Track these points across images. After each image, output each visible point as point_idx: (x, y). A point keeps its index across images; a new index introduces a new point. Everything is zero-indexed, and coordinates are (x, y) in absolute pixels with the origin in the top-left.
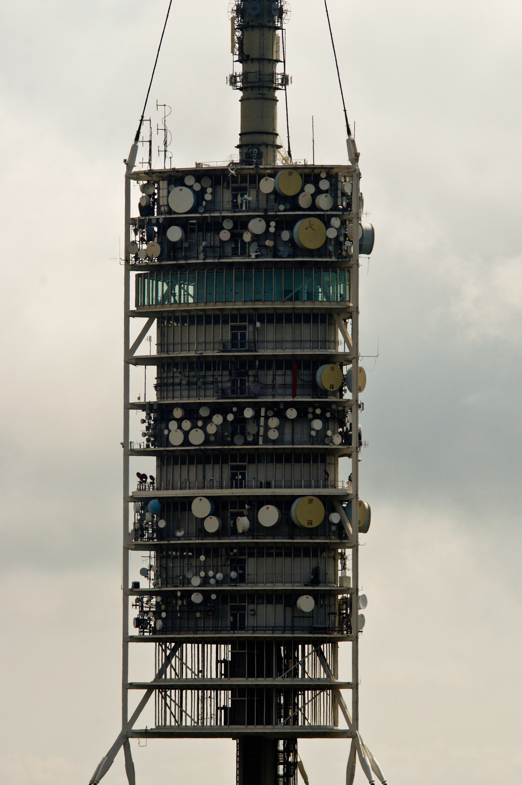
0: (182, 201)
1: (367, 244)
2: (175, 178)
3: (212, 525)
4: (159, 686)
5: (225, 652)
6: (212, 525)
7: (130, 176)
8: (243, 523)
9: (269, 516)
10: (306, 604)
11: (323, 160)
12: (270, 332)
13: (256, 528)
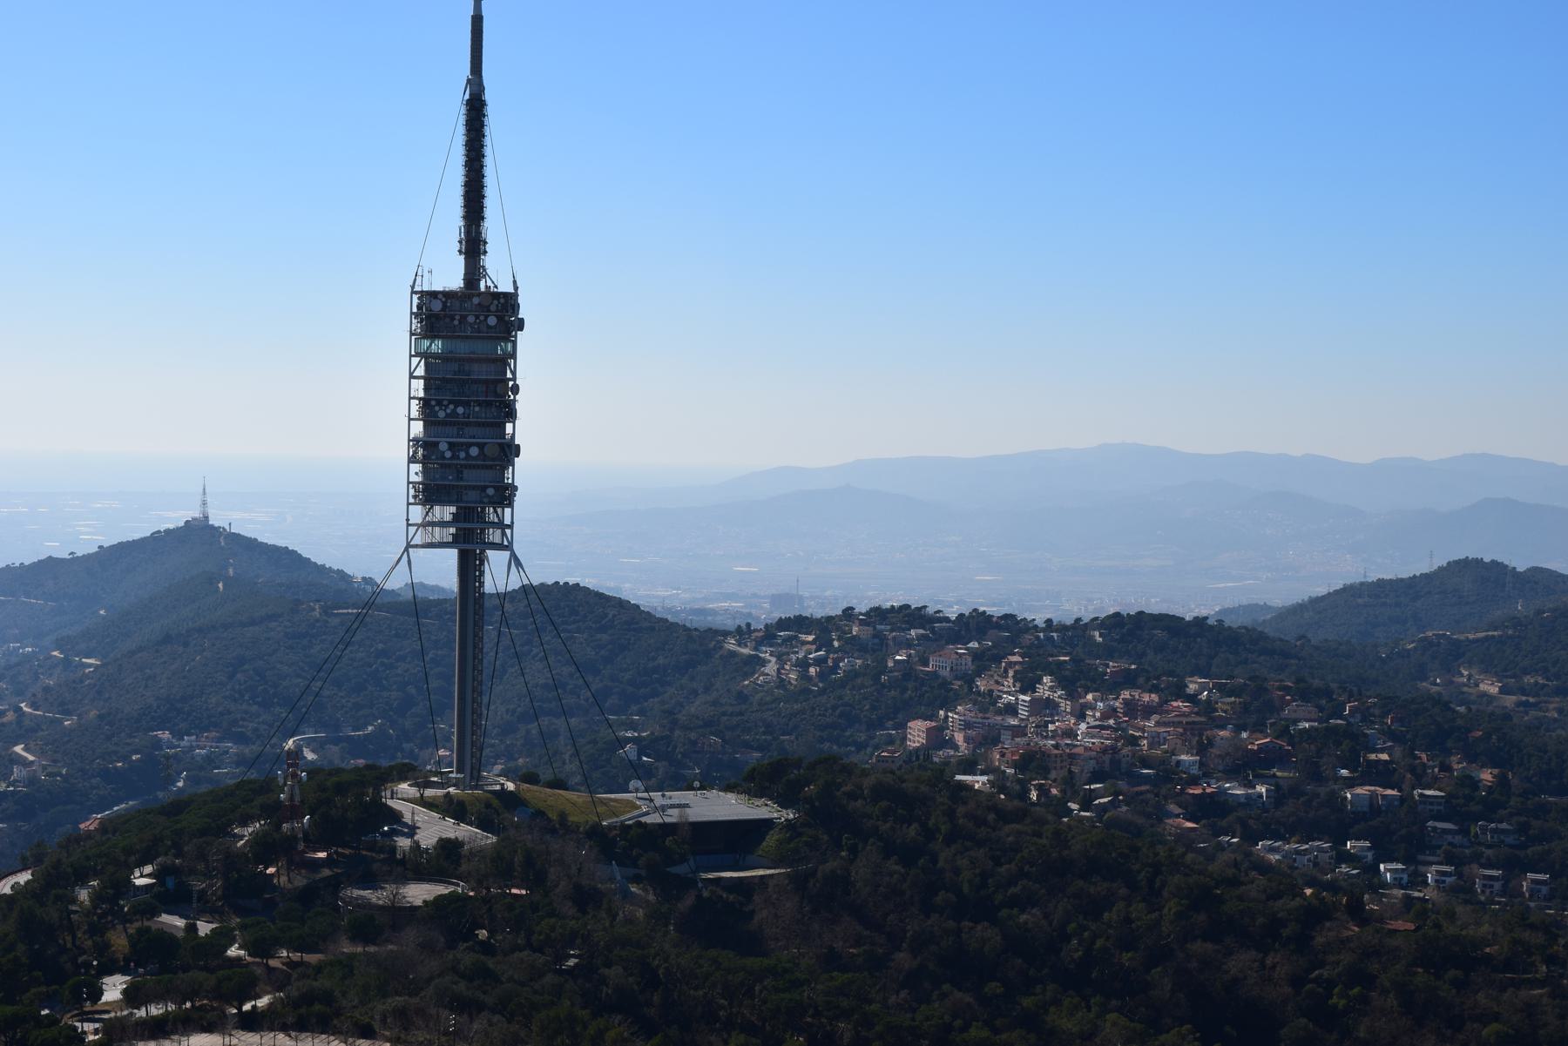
0: (437, 306)
1: (520, 325)
2: (433, 295)
3: (448, 454)
4: (425, 525)
5: (453, 509)
6: (448, 454)
7: (413, 292)
8: (462, 455)
9: (474, 451)
10: (491, 491)
11: (500, 290)
12: (476, 367)
13: (468, 456)
